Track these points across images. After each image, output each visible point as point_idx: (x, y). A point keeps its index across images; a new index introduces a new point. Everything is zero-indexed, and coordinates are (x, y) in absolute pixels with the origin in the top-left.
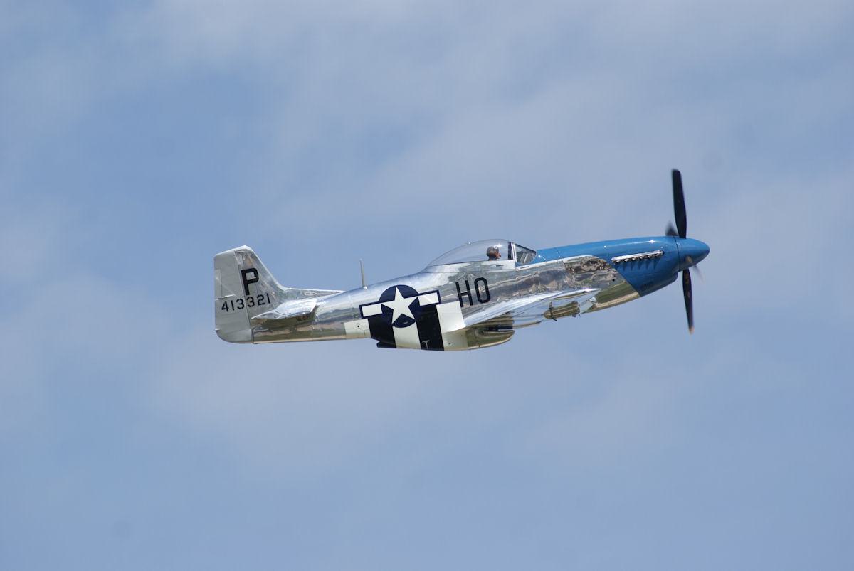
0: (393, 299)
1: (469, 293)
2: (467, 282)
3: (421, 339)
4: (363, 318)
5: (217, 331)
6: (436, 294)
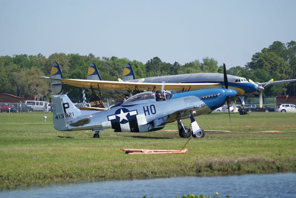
1: (148, 110)
3: (131, 128)
4: (109, 120)
5: (54, 127)
6: (136, 111)
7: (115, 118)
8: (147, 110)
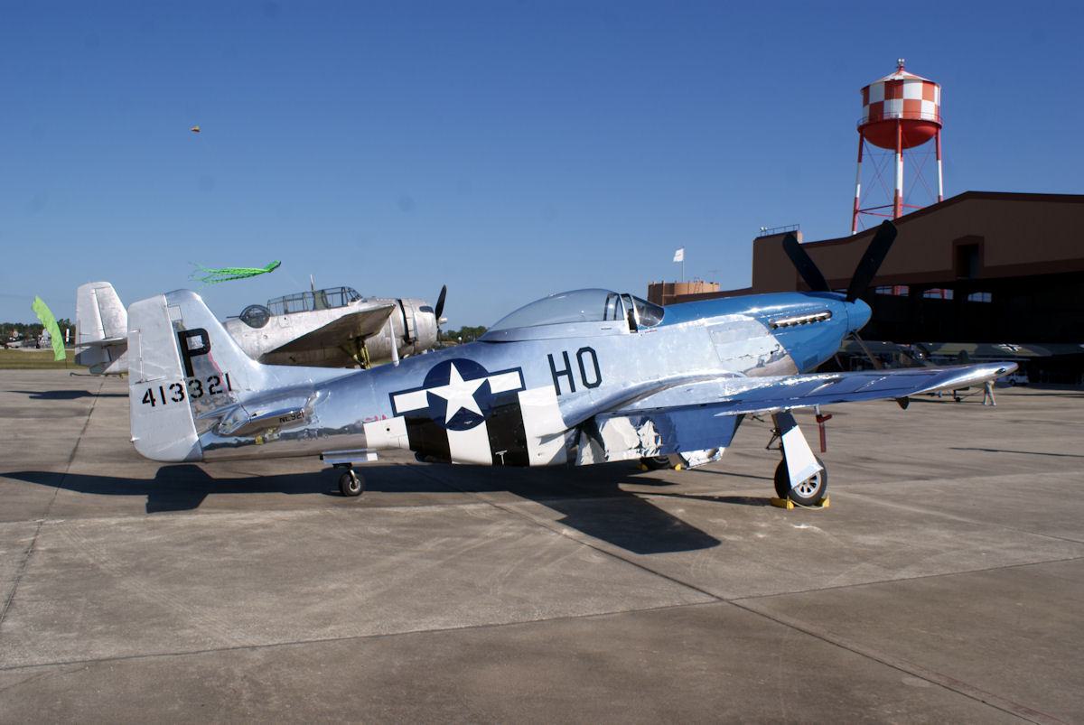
0: (446, 382)
1: (568, 372)
2: (565, 354)
3: (494, 447)
4: (396, 415)
6: (517, 373)
7: (427, 405)
8: (564, 368)
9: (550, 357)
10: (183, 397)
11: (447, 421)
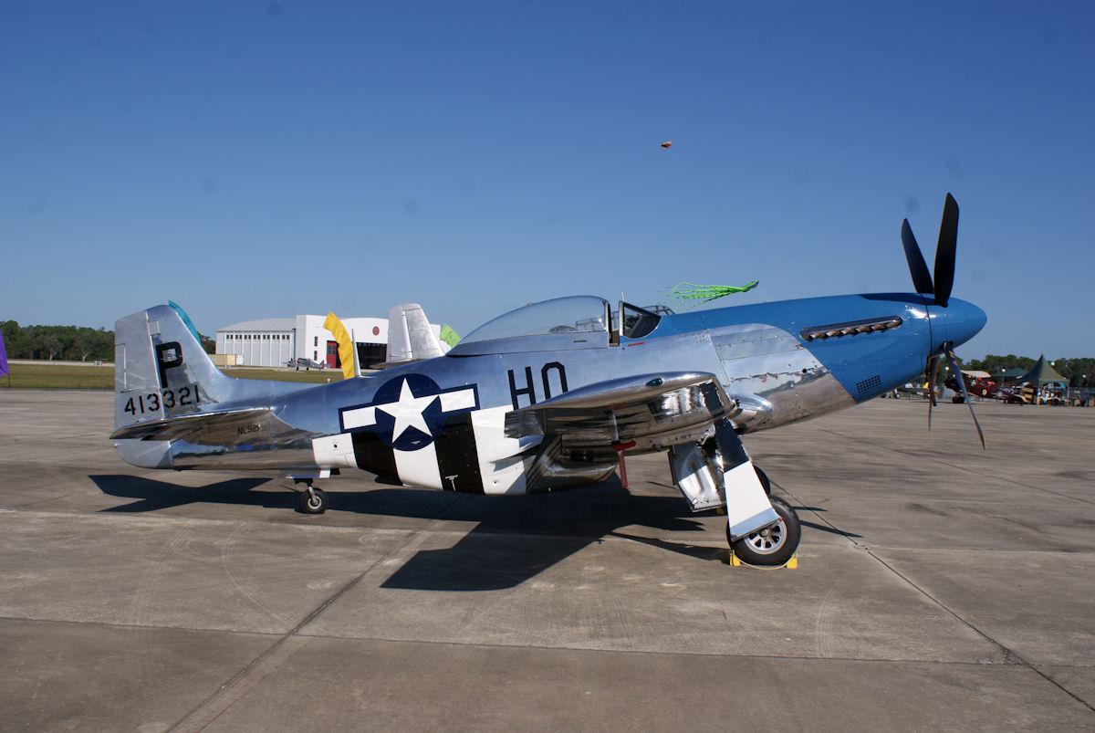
0: (395, 398)
1: (530, 390)
2: (528, 370)
4: (344, 431)
6: (471, 391)
7: (372, 421)
8: (525, 385)
9: (511, 373)
10: (158, 407)
11: (395, 437)
